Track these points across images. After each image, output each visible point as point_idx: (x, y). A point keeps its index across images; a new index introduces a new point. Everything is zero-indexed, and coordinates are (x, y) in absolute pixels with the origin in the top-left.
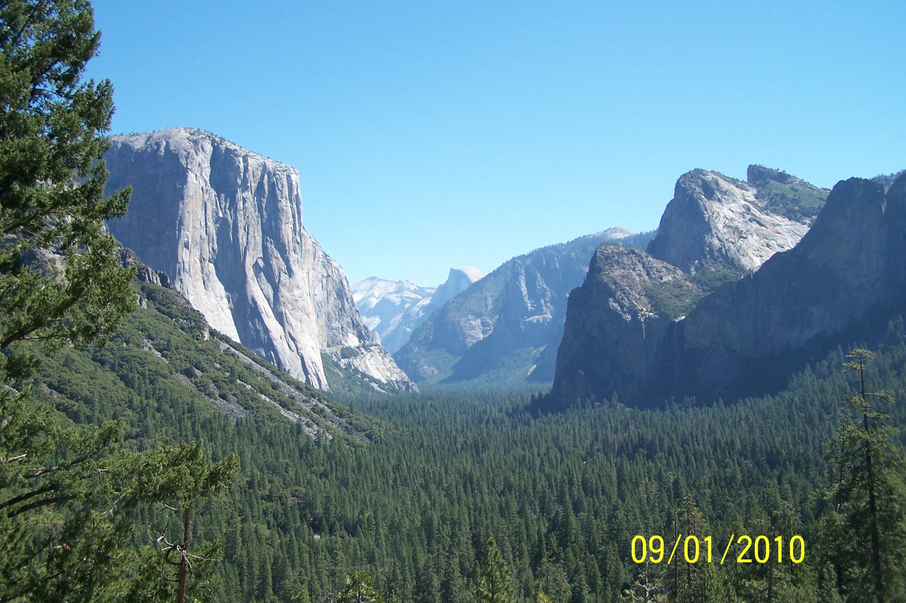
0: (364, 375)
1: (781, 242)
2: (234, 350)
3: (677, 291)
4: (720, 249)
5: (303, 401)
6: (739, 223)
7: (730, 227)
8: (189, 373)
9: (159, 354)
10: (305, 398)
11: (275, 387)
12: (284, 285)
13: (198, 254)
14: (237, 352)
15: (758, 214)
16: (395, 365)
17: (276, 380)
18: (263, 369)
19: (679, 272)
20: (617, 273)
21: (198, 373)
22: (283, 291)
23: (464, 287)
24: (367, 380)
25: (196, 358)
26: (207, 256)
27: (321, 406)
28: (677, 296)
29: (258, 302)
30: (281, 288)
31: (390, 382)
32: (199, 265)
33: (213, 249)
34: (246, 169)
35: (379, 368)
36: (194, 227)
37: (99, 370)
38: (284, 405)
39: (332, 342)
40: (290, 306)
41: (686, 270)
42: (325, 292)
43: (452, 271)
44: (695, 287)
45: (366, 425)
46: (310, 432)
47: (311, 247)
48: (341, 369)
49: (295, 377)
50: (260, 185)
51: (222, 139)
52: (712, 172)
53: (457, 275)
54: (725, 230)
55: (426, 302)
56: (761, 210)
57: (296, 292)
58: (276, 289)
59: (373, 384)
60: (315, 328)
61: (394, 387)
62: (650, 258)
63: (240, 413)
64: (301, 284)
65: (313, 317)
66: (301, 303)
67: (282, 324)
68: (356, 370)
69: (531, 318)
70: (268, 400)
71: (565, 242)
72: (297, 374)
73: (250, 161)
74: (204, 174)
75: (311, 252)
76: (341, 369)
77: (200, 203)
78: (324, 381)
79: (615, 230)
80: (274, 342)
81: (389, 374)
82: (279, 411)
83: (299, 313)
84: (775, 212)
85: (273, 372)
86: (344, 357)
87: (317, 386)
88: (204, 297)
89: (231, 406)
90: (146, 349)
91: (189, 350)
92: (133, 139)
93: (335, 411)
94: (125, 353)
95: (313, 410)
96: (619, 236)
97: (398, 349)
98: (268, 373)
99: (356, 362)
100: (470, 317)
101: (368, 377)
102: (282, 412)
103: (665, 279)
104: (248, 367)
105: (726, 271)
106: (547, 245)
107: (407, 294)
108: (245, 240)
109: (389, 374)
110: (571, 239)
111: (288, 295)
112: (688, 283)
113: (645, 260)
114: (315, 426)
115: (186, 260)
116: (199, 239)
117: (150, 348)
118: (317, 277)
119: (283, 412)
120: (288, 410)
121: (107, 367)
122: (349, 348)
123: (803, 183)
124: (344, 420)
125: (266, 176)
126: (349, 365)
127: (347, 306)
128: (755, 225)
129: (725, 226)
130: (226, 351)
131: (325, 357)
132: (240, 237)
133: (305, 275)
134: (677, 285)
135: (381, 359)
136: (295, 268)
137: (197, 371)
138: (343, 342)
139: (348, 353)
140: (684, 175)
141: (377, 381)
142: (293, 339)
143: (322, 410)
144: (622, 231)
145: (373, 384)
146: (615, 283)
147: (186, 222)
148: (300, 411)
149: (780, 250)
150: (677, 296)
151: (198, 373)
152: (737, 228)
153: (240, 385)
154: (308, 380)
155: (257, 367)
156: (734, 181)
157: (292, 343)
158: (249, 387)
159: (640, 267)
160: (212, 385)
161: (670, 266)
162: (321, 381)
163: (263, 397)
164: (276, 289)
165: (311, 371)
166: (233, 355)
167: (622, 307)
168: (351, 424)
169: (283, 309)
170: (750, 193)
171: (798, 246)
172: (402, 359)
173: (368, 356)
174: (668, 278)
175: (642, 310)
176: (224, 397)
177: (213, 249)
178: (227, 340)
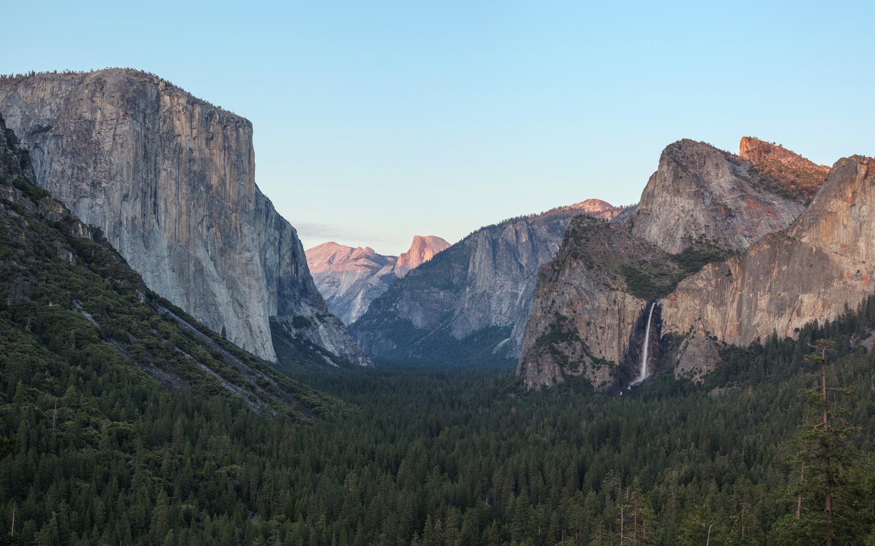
0: (317, 347)
1: (775, 222)
2: (173, 315)
3: (656, 271)
4: (707, 226)
6: (728, 200)
7: (719, 204)
8: (120, 338)
9: (88, 316)
10: (249, 370)
11: (217, 356)
12: (232, 247)
13: (138, 207)
14: (177, 318)
15: (750, 190)
16: (350, 337)
17: (219, 350)
18: (205, 337)
21: (133, 339)
23: (428, 256)
25: (129, 322)
26: (150, 210)
27: (267, 379)
28: (656, 276)
31: (343, 356)
32: (139, 221)
33: (155, 204)
36: (133, 179)
37: (20, 332)
38: (225, 376)
39: (282, 310)
42: (277, 256)
44: (676, 267)
45: (314, 401)
46: (255, 408)
47: (263, 207)
49: (241, 347)
51: (168, 85)
52: (703, 143)
53: (422, 243)
54: (712, 207)
55: (385, 271)
56: (754, 186)
57: (247, 255)
58: (223, 252)
59: (325, 357)
60: (266, 298)
61: (348, 362)
63: (178, 384)
65: (264, 283)
66: (250, 267)
68: (308, 342)
69: (498, 293)
70: (208, 370)
71: (538, 213)
74: (147, 121)
77: (141, 152)
79: (594, 201)
80: (220, 308)
81: (343, 347)
84: (768, 189)
85: (216, 341)
86: (296, 327)
88: (143, 256)
89: (167, 377)
90: (75, 311)
91: (123, 313)
92: (69, 77)
94: (51, 314)
95: (257, 382)
96: (599, 209)
97: (354, 321)
98: (209, 341)
99: (308, 333)
100: (433, 289)
102: (223, 384)
103: (645, 258)
104: (188, 335)
105: (713, 250)
106: (519, 216)
109: (343, 347)
110: (545, 210)
112: (669, 263)
114: (258, 400)
115: (125, 215)
116: (140, 194)
117: (79, 311)
118: (269, 240)
120: (233, 382)
121: (28, 328)
122: (301, 318)
123: (800, 158)
126: (300, 336)
127: (301, 270)
128: (744, 204)
129: (714, 203)
130: (165, 318)
131: (274, 326)
133: (255, 236)
134: (656, 265)
135: (335, 331)
136: (245, 230)
137: (130, 336)
138: (295, 311)
139: (301, 322)
142: (241, 306)
144: (602, 203)
145: (325, 357)
147: (125, 172)
149: (770, 230)
150: (656, 276)
151: (133, 339)
152: (725, 207)
153: (177, 353)
154: (256, 350)
155: (199, 334)
156: (726, 155)
157: (238, 309)
158: (188, 356)
160: (148, 353)
162: (268, 354)
163: (203, 367)
164: (223, 252)
166: (173, 321)
168: (298, 399)
169: (230, 272)
170: (741, 168)
171: (792, 225)
173: (321, 327)
175: (618, 289)
176: (159, 365)
177: (155, 204)
178: (165, 303)
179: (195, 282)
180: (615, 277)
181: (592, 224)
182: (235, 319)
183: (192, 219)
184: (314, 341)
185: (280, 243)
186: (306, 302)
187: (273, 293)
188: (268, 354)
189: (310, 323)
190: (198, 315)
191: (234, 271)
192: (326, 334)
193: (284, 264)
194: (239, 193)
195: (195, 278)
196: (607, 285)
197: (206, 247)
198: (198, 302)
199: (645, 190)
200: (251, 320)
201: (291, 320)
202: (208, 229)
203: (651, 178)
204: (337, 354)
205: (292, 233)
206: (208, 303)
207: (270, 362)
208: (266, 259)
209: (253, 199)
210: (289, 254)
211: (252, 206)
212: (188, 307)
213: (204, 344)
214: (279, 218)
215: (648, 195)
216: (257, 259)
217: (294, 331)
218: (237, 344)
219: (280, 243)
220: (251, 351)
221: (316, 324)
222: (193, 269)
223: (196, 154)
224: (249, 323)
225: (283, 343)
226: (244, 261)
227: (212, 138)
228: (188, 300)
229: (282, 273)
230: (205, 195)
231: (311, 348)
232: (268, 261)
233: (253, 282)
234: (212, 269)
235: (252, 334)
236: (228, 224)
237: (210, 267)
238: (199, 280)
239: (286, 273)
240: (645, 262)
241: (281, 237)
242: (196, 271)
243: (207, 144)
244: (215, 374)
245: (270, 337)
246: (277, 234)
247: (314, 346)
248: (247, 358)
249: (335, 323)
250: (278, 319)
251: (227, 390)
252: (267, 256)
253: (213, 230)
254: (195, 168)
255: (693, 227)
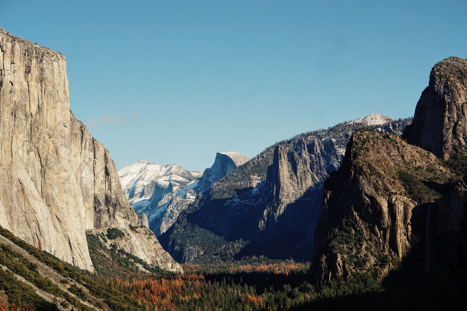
5: (62, 282)
11: (33, 267)
16: (160, 246)
19: (433, 157)
20: (372, 156)
22: (49, 173)
24: (133, 260)
27: (79, 286)
29: (25, 185)
30: (47, 170)
34: (13, 52)
35: (144, 249)
38: (40, 285)
40: (56, 189)
41: (440, 155)
42: (93, 175)
43: (219, 156)
44: (449, 172)
47: (79, 132)
48: (107, 251)
50: (28, 71)
57: (64, 175)
61: (158, 267)
62: (404, 143)
64: (67, 166)
66: (67, 185)
67: (49, 206)
68: (122, 251)
70: (24, 280)
71: (326, 128)
72: (63, 254)
73: (17, 46)
75: (79, 136)
76: (107, 251)
78: (89, 262)
80: (41, 224)
82: (34, 291)
83: (64, 196)
87: (82, 267)
93: (92, 291)
98: (26, 254)
101: (134, 258)
102: (39, 292)
103: (418, 164)
107: (175, 177)
108: (12, 124)
109: (154, 255)
111: (55, 177)
113: (399, 145)
114: (70, 307)
119: (39, 292)
120: (45, 290)
122: (115, 230)
124: (101, 300)
125: (34, 61)
126: (114, 246)
132: (6, 120)
136: (63, 151)
138: (109, 223)
139: (114, 234)
140: (439, 64)
141: (140, 261)
143: (80, 290)
146: (370, 166)
148: (56, 291)
159: (394, 152)
161: (425, 152)
162: (85, 263)
163: (19, 278)
164: (43, 173)
165: (76, 252)
167: (377, 190)
169: (49, 191)
172: (165, 240)
173: (134, 237)
174: (423, 164)
175: (396, 193)
179: (18, 201)
180: (394, 182)
181: (372, 136)
182: (55, 233)
183: (14, 144)
184: (127, 250)
185: (95, 163)
186: (119, 216)
187: (89, 209)
188: (85, 263)
189: (124, 235)
190: (21, 231)
191: (53, 189)
192: (138, 243)
193: (98, 182)
194: (55, 119)
195: (18, 198)
196: (386, 189)
197: (27, 169)
198: (21, 219)
199: (418, 103)
200: (69, 233)
201: (106, 233)
202: (28, 152)
203: (423, 93)
204: (149, 262)
205: (105, 155)
206: (30, 220)
207: (87, 272)
208: (82, 178)
209: (68, 125)
210: (103, 172)
211: (67, 131)
212: (11, 224)
213: (19, 256)
214: (93, 140)
215: (420, 108)
216: (73, 178)
217: (109, 242)
218: (56, 256)
219: (95, 163)
220: (70, 262)
221: (128, 235)
222: (16, 189)
223: (17, 87)
224: (66, 237)
225: (100, 254)
226: (62, 181)
227: (29, 72)
228: (12, 217)
229: (96, 189)
230: (24, 122)
231: (125, 256)
232: (84, 180)
233: (71, 200)
234: (33, 188)
235: (71, 246)
236: (46, 148)
237: (30, 186)
238: (22, 199)
239: (101, 190)
240: (419, 167)
241: (95, 158)
242: (18, 191)
243: (26, 78)
244: (29, 283)
245: (87, 248)
246: (92, 154)
247: (127, 254)
248: (61, 266)
249: (146, 233)
250: (94, 233)
251: (41, 298)
252: (83, 176)
253: (32, 154)
254: (15, 99)
255: (461, 134)
